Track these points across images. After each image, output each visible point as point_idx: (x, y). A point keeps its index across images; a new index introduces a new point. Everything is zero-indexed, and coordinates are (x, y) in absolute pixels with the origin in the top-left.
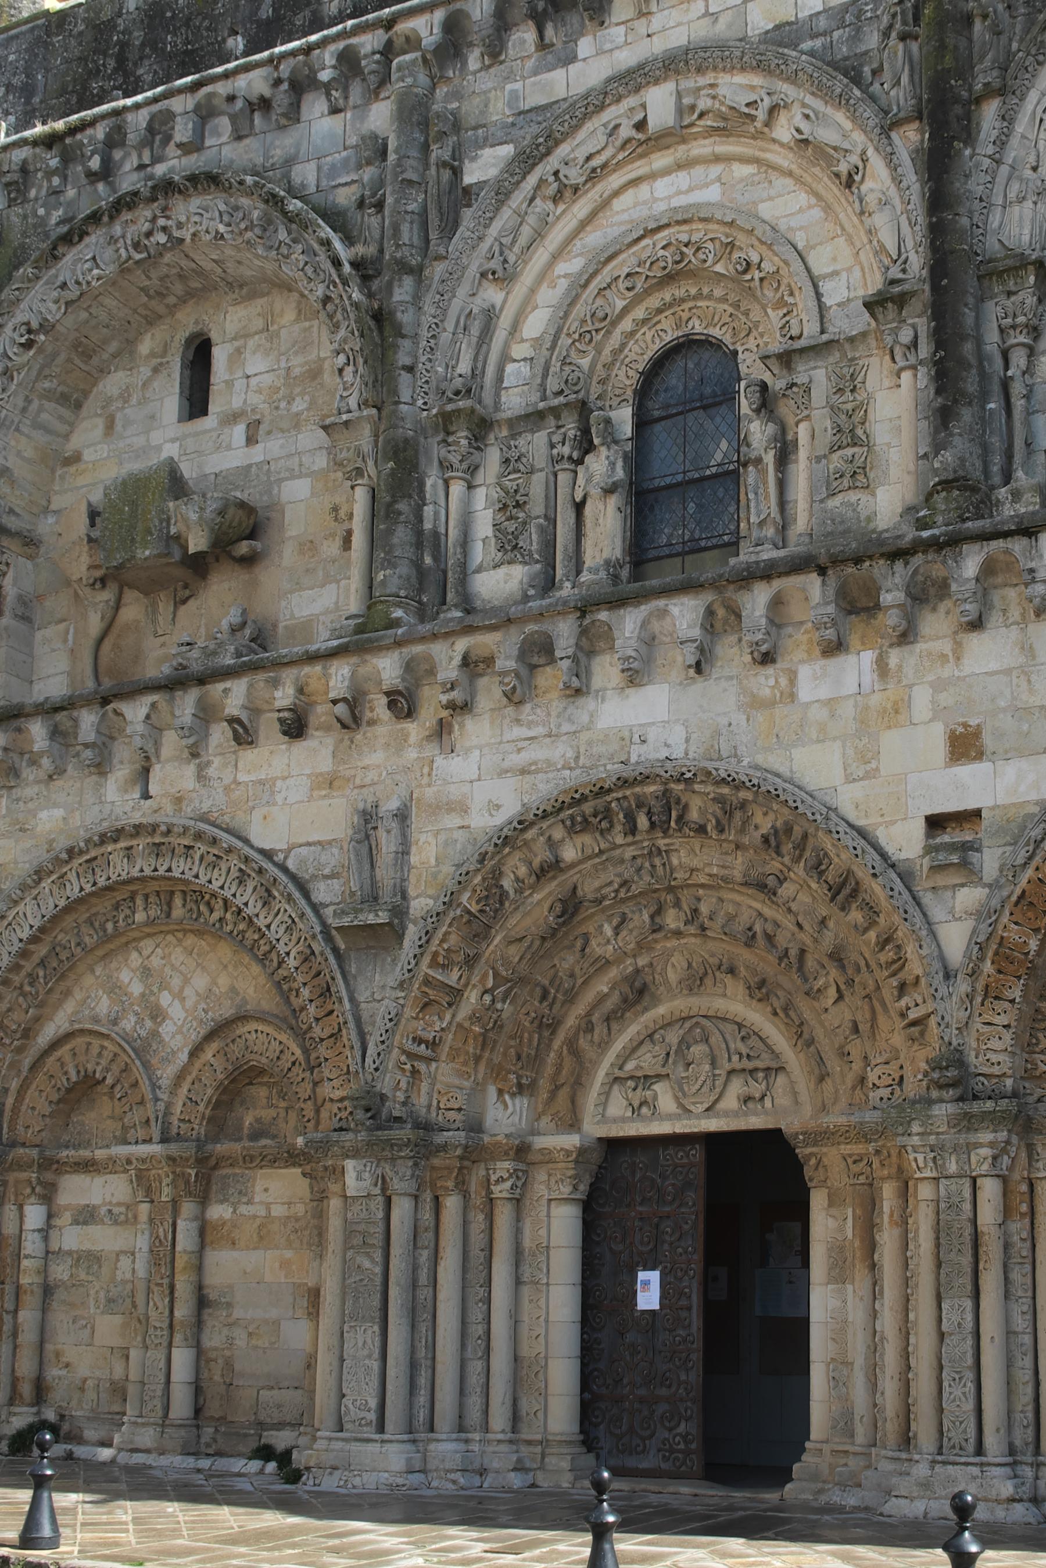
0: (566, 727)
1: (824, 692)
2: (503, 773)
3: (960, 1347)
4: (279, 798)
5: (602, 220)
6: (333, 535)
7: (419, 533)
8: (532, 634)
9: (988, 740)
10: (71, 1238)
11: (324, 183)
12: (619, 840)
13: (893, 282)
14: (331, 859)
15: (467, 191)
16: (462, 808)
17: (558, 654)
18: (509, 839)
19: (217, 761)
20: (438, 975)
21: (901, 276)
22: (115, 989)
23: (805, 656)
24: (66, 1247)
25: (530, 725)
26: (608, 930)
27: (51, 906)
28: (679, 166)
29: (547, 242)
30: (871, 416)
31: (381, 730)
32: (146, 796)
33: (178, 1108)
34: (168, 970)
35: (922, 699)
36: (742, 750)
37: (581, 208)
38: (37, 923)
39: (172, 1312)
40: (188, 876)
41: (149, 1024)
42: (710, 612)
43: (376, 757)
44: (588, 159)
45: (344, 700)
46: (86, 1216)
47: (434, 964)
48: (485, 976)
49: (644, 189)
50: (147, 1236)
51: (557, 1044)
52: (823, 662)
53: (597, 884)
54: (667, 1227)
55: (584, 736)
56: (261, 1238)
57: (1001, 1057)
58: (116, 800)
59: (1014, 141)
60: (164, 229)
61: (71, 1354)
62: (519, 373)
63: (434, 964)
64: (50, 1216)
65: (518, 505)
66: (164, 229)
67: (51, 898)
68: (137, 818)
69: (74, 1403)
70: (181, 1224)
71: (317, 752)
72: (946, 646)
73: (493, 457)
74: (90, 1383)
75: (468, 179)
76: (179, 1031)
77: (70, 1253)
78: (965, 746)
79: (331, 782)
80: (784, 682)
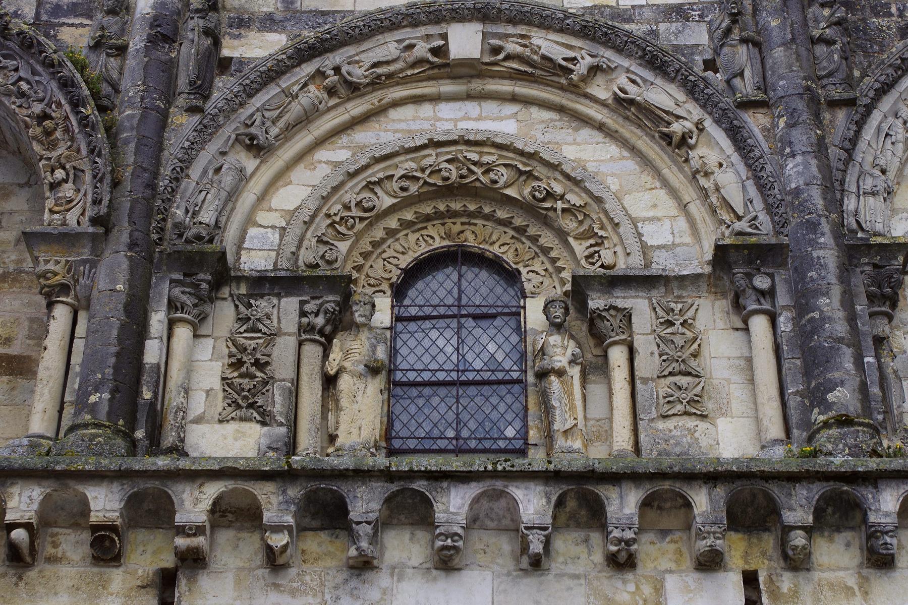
5: (373, 124)
8: (315, 491)
11: (44, 17)
13: (740, 234)
17: (353, 516)
21: (749, 230)
23: (673, 566)
28: (470, 97)
29: (312, 127)
30: (705, 351)
42: (560, 503)
44: (376, 65)
45: (27, 526)
49: (426, 110)
52: (697, 575)
59: (862, 145)
72: (852, 581)
75: (226, 52)
80: (647, 590)
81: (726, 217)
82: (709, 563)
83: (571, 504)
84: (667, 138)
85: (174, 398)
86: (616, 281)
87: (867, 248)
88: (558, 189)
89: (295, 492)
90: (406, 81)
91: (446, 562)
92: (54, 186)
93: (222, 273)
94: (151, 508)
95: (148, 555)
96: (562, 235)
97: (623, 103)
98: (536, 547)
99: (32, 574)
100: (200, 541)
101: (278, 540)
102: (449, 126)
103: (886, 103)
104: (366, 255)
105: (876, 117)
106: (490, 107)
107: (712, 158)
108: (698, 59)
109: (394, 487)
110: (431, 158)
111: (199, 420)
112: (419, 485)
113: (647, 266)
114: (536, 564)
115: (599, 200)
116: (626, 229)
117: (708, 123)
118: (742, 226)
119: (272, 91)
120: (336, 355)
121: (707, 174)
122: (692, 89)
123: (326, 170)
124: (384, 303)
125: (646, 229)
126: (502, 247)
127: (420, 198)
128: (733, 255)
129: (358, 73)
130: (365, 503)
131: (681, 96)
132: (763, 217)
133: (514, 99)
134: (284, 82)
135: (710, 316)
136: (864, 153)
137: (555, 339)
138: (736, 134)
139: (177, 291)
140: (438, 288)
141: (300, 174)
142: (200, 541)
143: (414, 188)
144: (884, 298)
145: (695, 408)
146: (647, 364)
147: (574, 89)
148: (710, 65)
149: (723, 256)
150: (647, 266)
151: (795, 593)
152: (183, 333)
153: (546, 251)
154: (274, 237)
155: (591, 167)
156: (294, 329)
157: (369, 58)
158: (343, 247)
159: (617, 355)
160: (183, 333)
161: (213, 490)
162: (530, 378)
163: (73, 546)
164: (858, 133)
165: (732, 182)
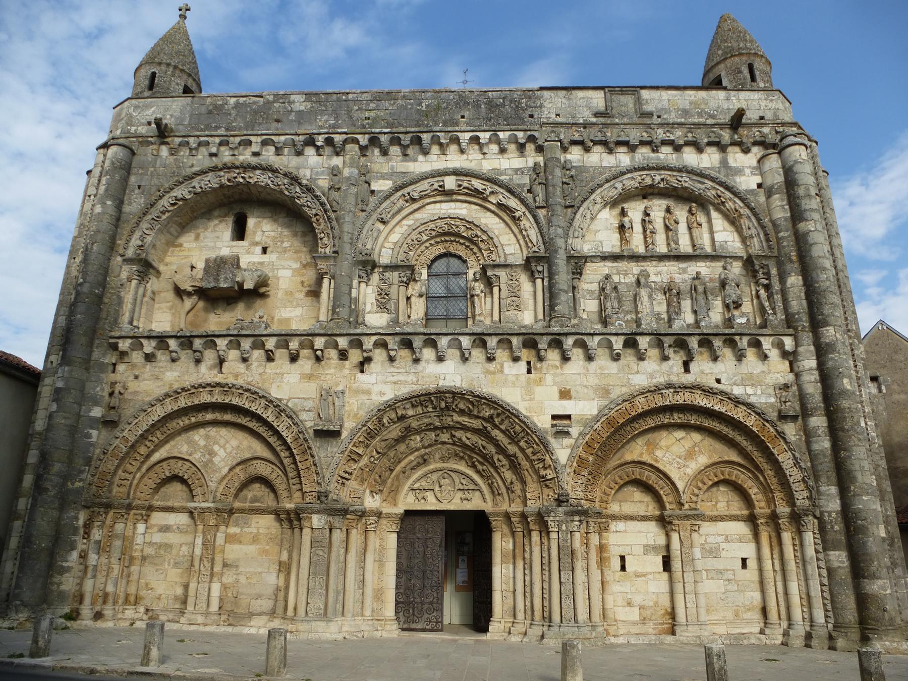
0: (413, 370)
1: (514, 371)
2: (386, 383)
3: (567, 587)
4: (285, 381)
5: (420, 211)
6: (301, 291)
7: (351, 298)
9: (573, 393)
10: (158, 538)
12: (431, 410)
14: (309, 404)
15: (373, 192)
16: (368, 392)
18: (391, 406)
19: (256, 364)
20: (354, 449)
22: (190, 442)
24: (154, 541)
25: (398, 368)
26: (418, 438)
27: (170, 408)
31: (332, 362)
32: (221, 372)
33: (221, 489)
34: (218, 437)
35: (549, 379)
36: (483, 386)
37: (416, 206)
38: (163, 415)
39: (212, 569)
40: (240, 404)
41: (207, 456)
42: (474, 341)
43: (332, 371)
46: (165, 529)
47: (354, 445)
48: (372, 451)
50: (201, 538)
51: (392, 476)
53: (419, 423)
54: (429, 542)
55: (421, 374)
56: (254, 541)
57: (581, 493)
58: (206, 373)
59: (576, 220)
60: (243, 178)
61: (153, 584)
62: (387, 252)
63: (354, 445)
64: (147, 528)
65: (386, 294)
66: (243, 178)
67: (170, 406)
68: (217, 380)
69: (154, 605)
70: (219, 534)
71: (306, 364)
72: (558, 364)
73: (375, 277)
74: (163, 596)
75: (373, 188)
76: (223, 460)
77: (156, 543)
78: (565, 394)
79: (310, 377)
80: (499, 367)
81: (530, 245)
82: (516, 359)
83: (477, 342)
84: (514, 217)
85: (361, 307)
86: (495, 266)
87: (574, 257)
88: (479, 234)
89: (397, 338)
90: (431, 196)
91: (440, 359)
92: (321, 239)
93: (374, 266)
94: (357, 343)
95: (355, 356)
96: (480, 249)
97: (500, 205)
98: (467, 355)
99: (323, 363)
100: (370, 354)
101: (392, 353)
102: (444, 211)
103: (585, 204)
104: (419, 256)
105: (581, 209)
106: (458, 204)
107: (528, 225)
108: (525, 189)
109: (426, 337)
110: (439, 223)
111: (369, 313)
112: (433, 337)
113: (506, 261)
114: (467, 359)
115: (492, 238)
116: (500, 248)
117: (527, 213)
118: (535, 249)
119: (388, 202)
120: (410, 292)
121: (526, 230)
122: (522, 201)
123: (406, 228)
124: (425, 273)
125: (506, 248)
126: (461, 252)
127: (436, 236)
128: (531, 260)
129: (416, 195)
130: (417, 342)
131: (519, 203)
132: (542, 246)
133: (466, 202)
134: (392, 199)
135: (524, 279)
136: (576, 223)
137: (477, 284)
138: (535, 217)
139: (361, 272)
140: (440, 266)
141: (397, 229)
142: (370, 354)
143: (434, 233)
144: (578, 273)
145: (518, 308)
146: (504, 294)
147: (485, 199)
148: (530, 191)
149: (528, 260)
150: (506, 261)
151: (541, 368)
152: (363, 285)
153: (475, 254)
154: (391, 251)
155: (490, 226)
156: (397, 282)
157: (419, 189)
158: (412, 253)
159: (496, 290)
160: (363, 285)
161: (374, 338)
162: (468, 296)
163: (333, 354)
164: (574, 217)
165: (533, 234)
